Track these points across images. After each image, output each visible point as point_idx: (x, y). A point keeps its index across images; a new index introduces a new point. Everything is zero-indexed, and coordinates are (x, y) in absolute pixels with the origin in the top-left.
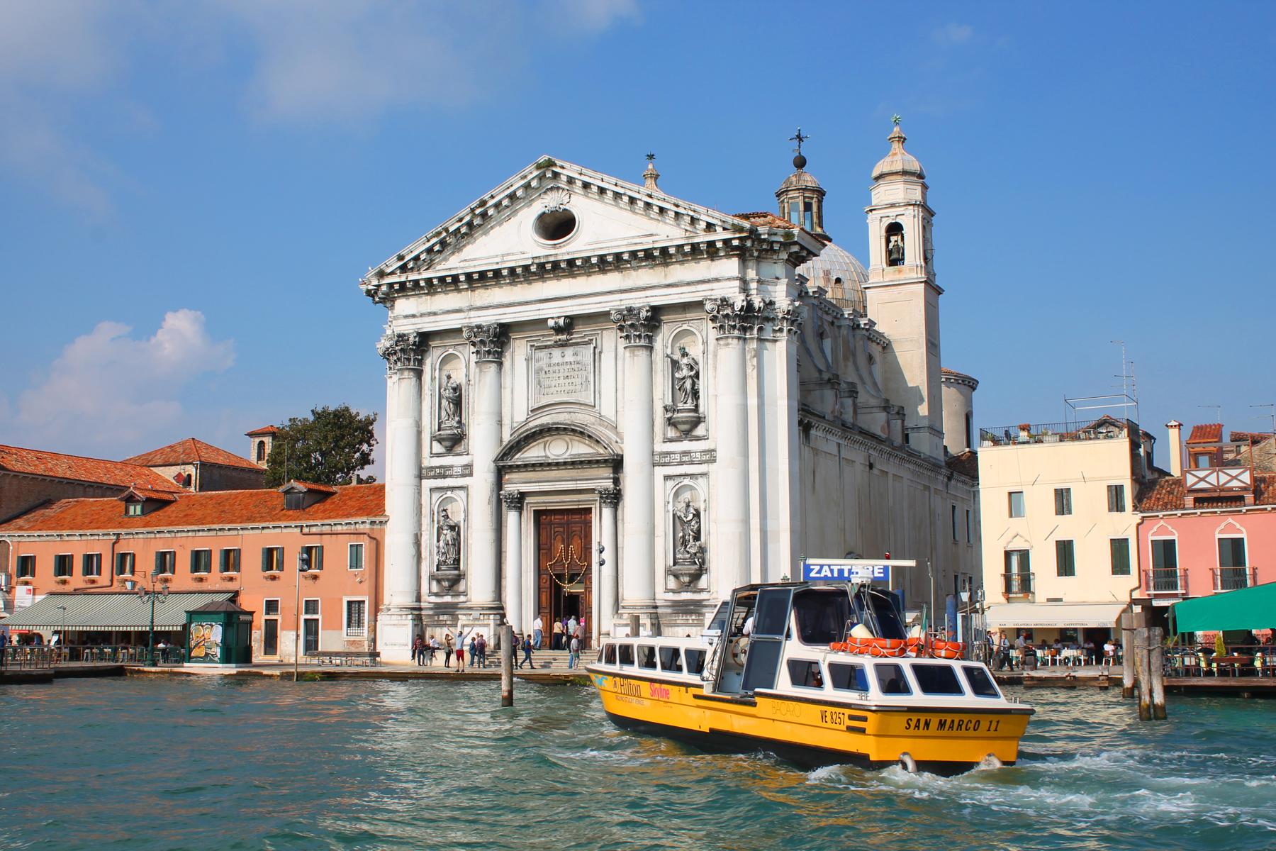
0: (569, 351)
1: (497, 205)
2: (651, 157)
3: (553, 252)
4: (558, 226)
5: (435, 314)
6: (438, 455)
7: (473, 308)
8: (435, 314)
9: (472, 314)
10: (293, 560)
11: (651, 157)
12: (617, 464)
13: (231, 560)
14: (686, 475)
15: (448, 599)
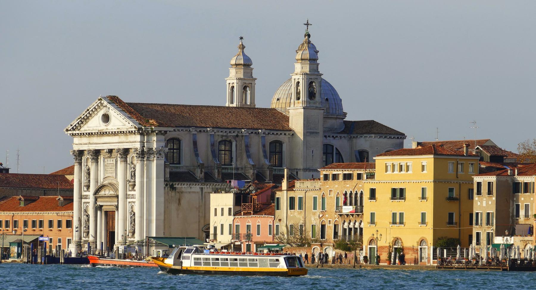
0: (111, 159)
1: (92, 110)
2: (241, 38)
3: (105, 128)
4: (106, 118)
5: (81, 144)
6: (85, 191)
7: (90, 143)
8: (81, 144)
9: (90, 145)
10: (55, 224)
11: (241, 38)
12: (117, 197)
13: (41, 223)
14: (132, 202)
15: (87, 239)
